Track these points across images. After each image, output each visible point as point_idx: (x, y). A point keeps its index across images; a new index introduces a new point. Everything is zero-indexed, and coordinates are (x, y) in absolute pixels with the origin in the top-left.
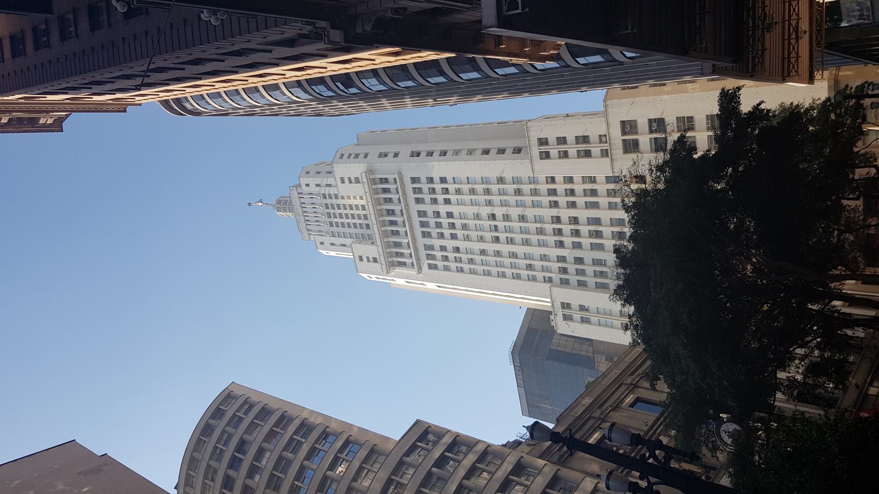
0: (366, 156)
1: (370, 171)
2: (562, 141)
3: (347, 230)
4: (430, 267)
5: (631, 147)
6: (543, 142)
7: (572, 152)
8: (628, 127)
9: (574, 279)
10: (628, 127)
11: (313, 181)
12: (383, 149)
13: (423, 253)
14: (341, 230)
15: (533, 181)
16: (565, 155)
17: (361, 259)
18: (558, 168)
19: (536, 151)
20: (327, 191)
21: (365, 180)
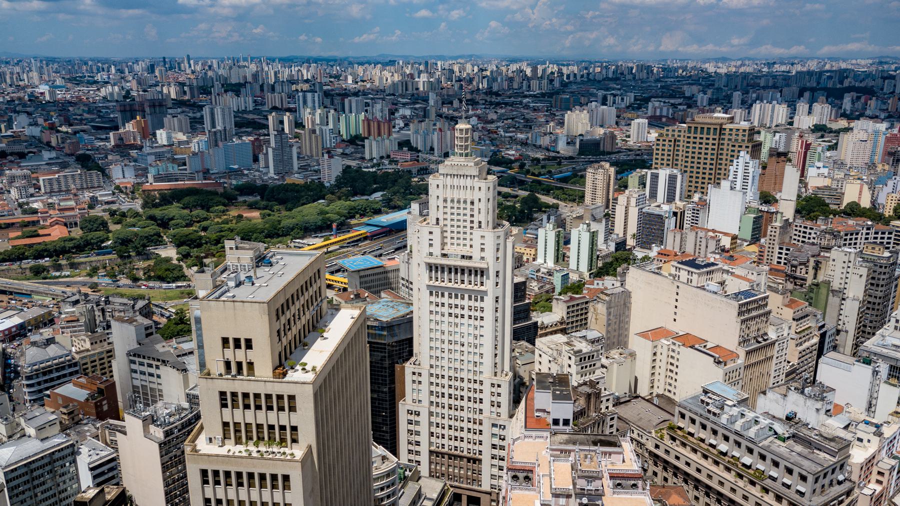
0: (498, 258)
9: (433, 379)
16: (492, 394)
17: (431, 233)
20: (476, 207)
21: (483, 265)
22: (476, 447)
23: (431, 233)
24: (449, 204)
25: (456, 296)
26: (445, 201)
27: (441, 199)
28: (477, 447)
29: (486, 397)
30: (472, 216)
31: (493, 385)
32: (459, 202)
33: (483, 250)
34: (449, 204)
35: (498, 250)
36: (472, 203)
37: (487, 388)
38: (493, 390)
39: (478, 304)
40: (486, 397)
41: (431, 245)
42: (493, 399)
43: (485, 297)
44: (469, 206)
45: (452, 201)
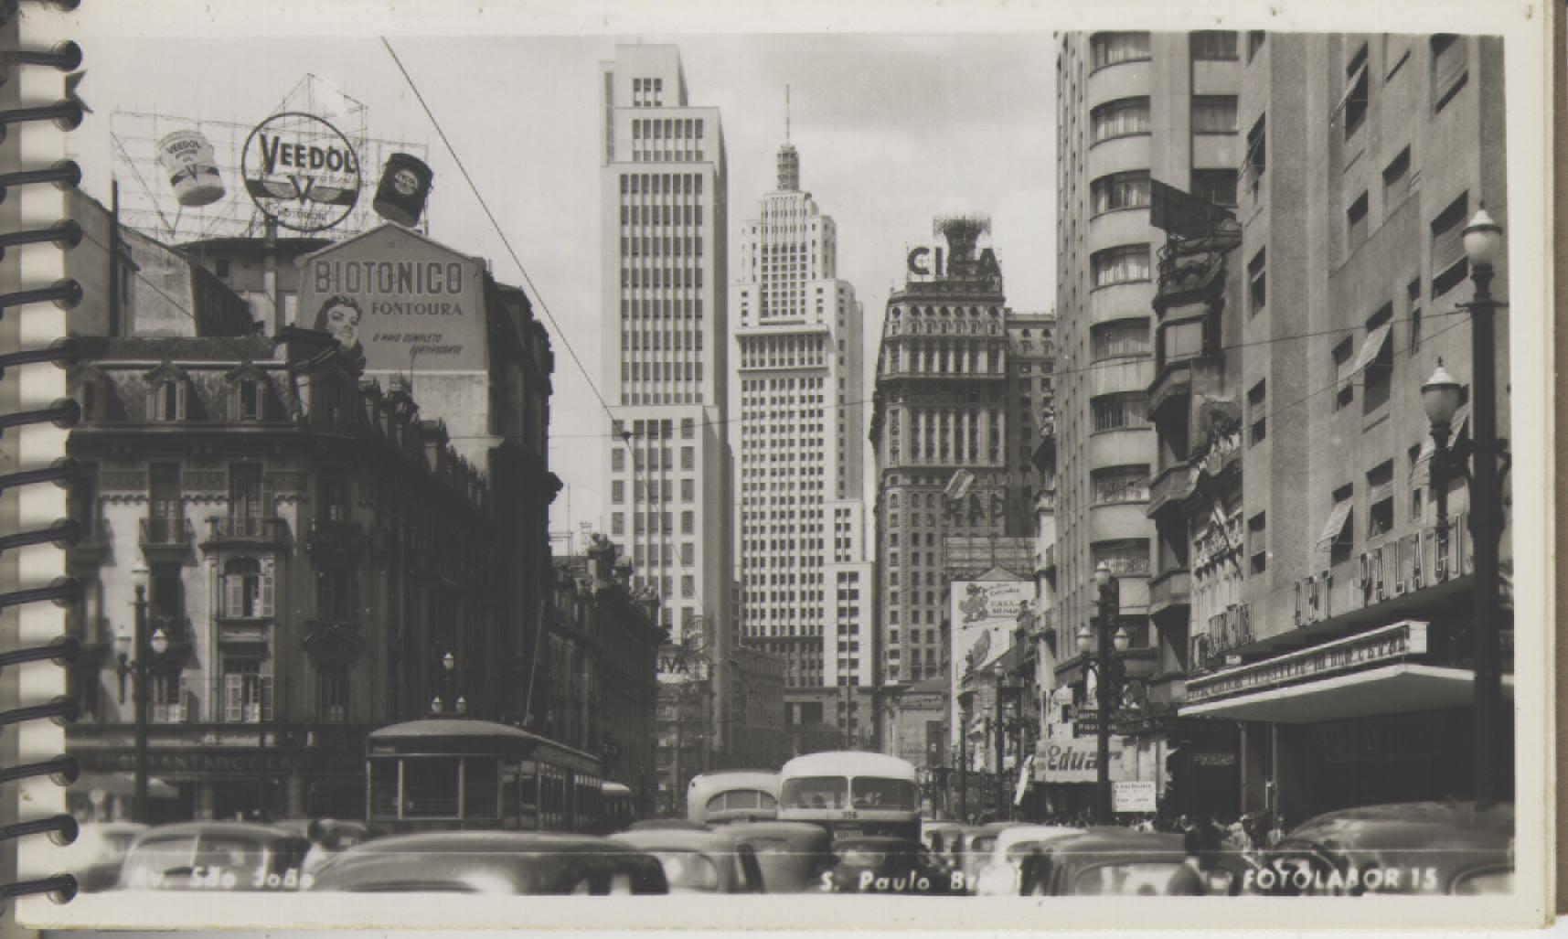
0: (841, 323)
1: (827, 334)
2: (848, 527)
3: (770, 273)
4: (744, 383)
5: (841, 577)
6: (847, 512)
7: (840, 535)
8: (854, 577)
10: (854, 577)
11: (818, 235)
12: (847, 344)
13: (757, 378)
14: (770, 264)
15: (820, 499)
16: (838, 527)
18: (829, 521)
19: (843, 505)
20: (809, 254)
21: (822, 328)
22: (814, 622)
23: (745, 294)
24: (770, 255)
25: (782, 386)
26: (765, 250)
27: (759, 247)
28: (814, 622)
29: (828, 535)
30: (804, 267)
31: (838, 513)
32: (784, 250)
33: (820, 310)
34: (770, 255)
35: (841, 310)
36: (803, 248)
37: (829, 521)
38: (839, 520)
39: (814, 392)
40: (828, 535)
41: (745, 313)
42: (840, 535)
43: (826, 381)
44: (798, 254)
45: (775, 250)
